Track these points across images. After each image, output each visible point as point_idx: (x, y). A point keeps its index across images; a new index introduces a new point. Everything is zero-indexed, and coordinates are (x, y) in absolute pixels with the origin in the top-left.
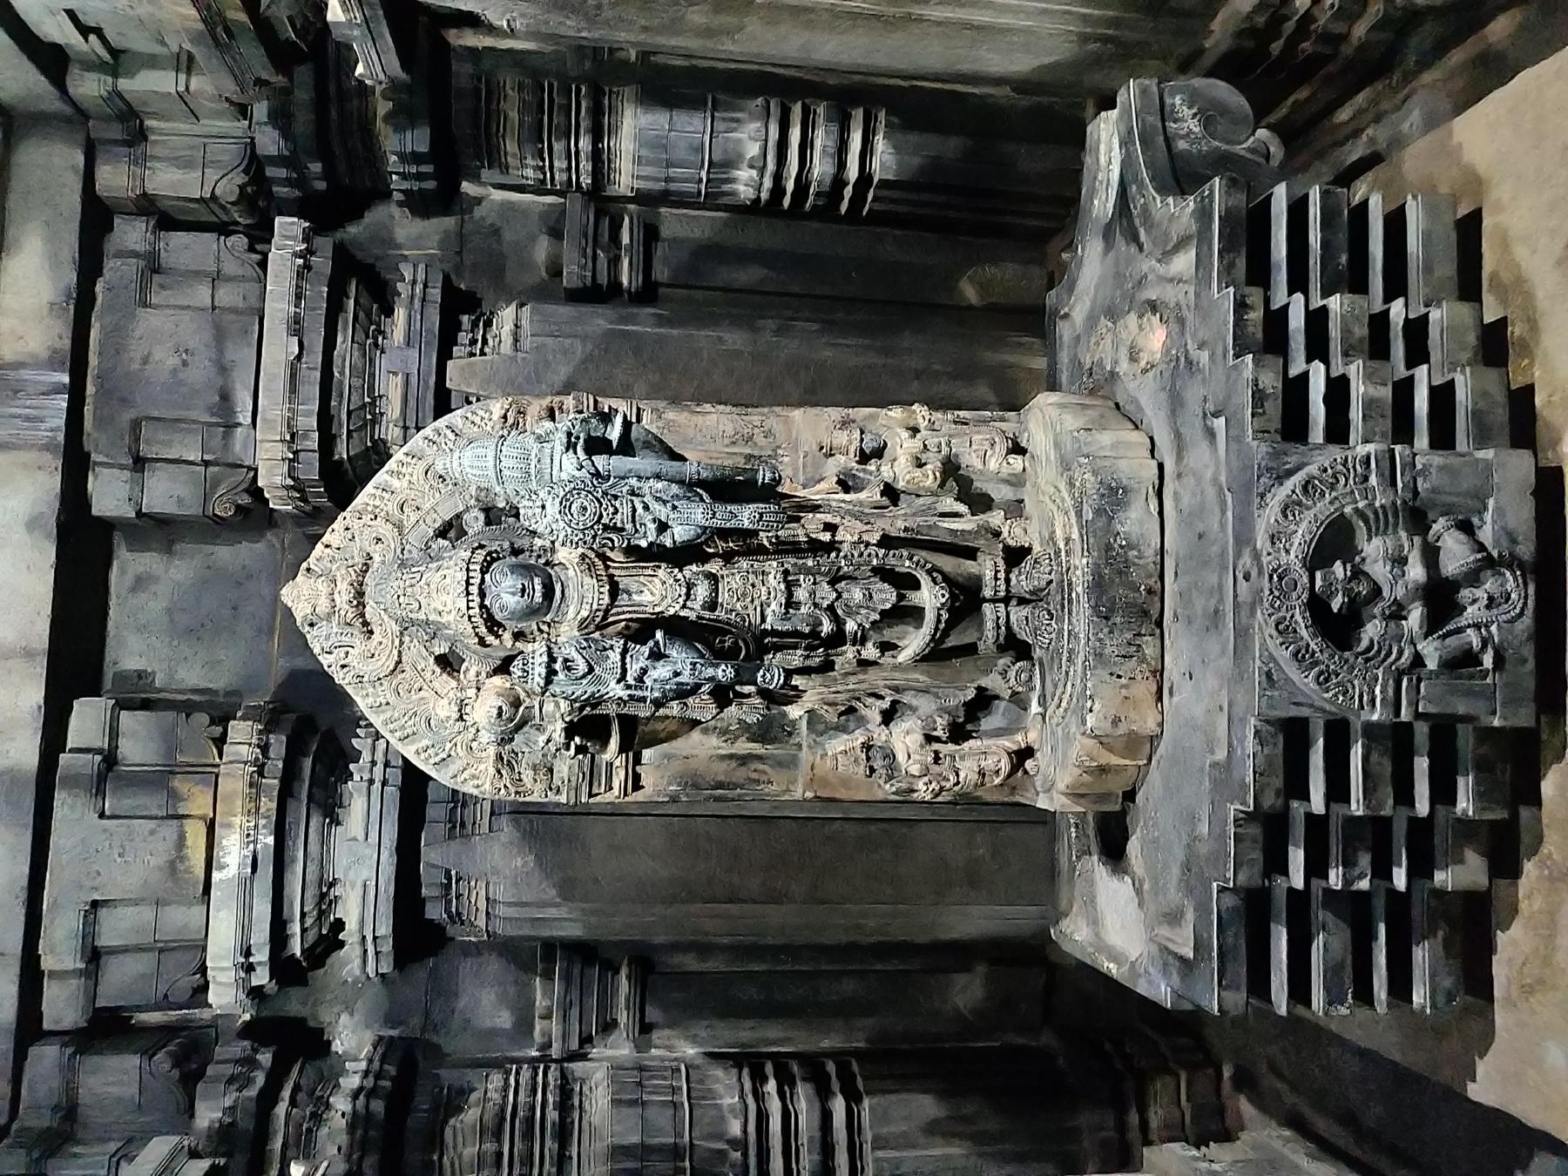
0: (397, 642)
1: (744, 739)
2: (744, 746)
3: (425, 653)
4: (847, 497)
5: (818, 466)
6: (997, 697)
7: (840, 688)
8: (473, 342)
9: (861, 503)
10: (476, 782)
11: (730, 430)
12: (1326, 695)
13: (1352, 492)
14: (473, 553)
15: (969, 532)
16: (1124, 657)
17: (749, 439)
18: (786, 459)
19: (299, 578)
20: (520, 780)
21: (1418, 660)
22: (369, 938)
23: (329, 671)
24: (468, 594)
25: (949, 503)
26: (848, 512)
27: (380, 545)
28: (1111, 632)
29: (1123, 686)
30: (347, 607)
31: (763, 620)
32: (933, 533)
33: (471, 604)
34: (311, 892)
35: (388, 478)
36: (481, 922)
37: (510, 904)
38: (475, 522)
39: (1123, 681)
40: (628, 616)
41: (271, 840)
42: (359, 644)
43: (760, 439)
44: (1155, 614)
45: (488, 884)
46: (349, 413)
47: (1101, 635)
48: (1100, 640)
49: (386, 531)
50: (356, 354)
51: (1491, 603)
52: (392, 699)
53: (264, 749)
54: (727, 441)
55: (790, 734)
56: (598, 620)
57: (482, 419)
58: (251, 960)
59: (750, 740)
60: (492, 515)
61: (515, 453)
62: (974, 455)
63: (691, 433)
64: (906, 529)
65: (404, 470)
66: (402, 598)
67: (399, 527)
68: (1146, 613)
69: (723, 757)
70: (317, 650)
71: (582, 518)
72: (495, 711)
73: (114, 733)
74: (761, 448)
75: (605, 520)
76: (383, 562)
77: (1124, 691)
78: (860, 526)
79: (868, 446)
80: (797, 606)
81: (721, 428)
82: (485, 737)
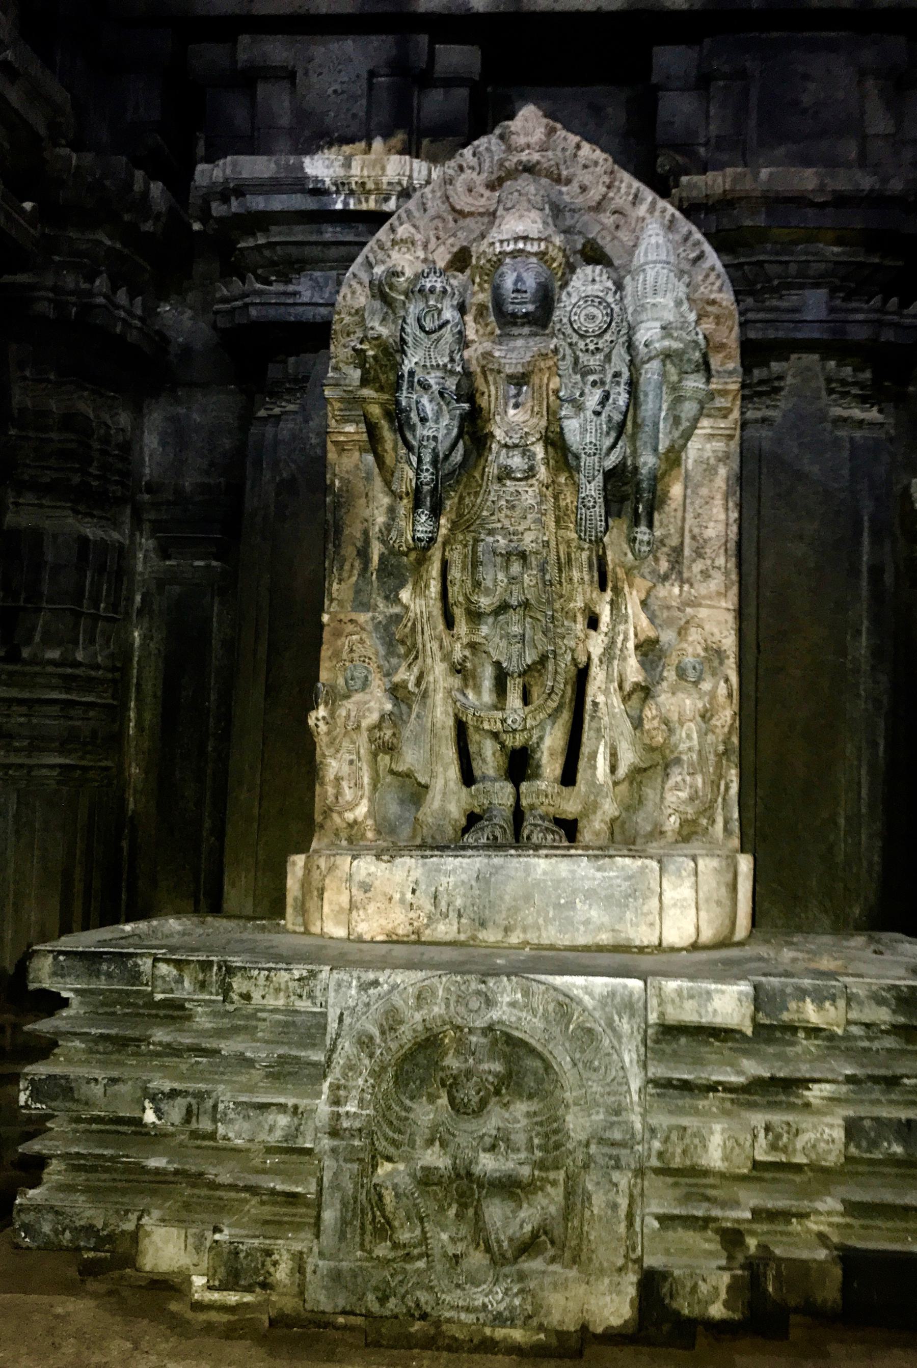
0: (481, 210)
1: (383, 550)
2: (376, 550)
3: (472, 237)
4: (631, 645)
6: (418, 810)
7: (426, 636)
8: (843, 383)
9: (624, 659)
10: (349, 296)
11: (710, 533)
12: (347, 1045)
13: (581, 1086)
14: (560, 248)
15: (594, 775)
16: (435, 898)
17: (699, 554)
18: (676, 590)
19: (545, 121)
20: (348, 335)
22: (247, 300)
23: (457, 156)
24: (516, 239)
25: (628, 758)
26: (613, 642)
27: (579, 191)
28: (463, 882)
29: (403, 894)
30: (515, 160)
31: (491, 532)
32: (592, 734)
33: (505, 244)
34: (294, 251)
35: (650, 199)
36: (262, 413)
37: (276, 436)
39: (409, 896)
40: (493, 392)
41: (339, 206)
42: (480, 180)
43: (698, 567)
45: (296, 412)
46: (760, 263)
47: (459, 871)
48: (454, 871)
49: (595, 193)
50: (823, 266)
52: (432, 212)
54: (696, 531)
55: (387, 598)
56: (490, 366)
57: (713, 284)
58: (233, 199)
59: (382, 557)
61: (662, 280)
62: (679, 778)
63: (704, 491)
64: (595, 704)
65: (657, 214)
66: (516, 194)
67: (598, 207)
68: (483, 924)
69: (366, 533)
70: (476, 143)
71: (582, 319)
72: (399, 269)
73: (449, 82)
74: (690, 568)
75: (581, 345)
76: (561, 193)
77: (397, 896)
81: (711, 524)
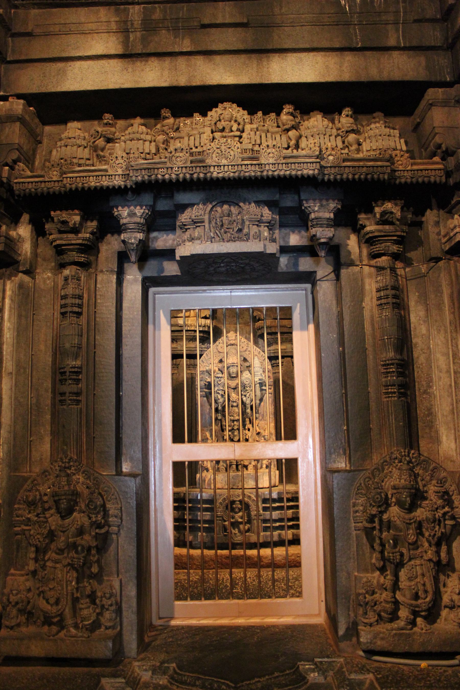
5: (262, 428)
21: (225, 521)
38: (247, 364)
44: (234, 487)
49: (245, 349)
51: (235, 534)
53: (204, 326)
60: (249, 367)
67: (245, 351)
68: (234, 485)
78: (250, 435)
79: (266, 437)
80: (233, 422)
82: (207, 368)
